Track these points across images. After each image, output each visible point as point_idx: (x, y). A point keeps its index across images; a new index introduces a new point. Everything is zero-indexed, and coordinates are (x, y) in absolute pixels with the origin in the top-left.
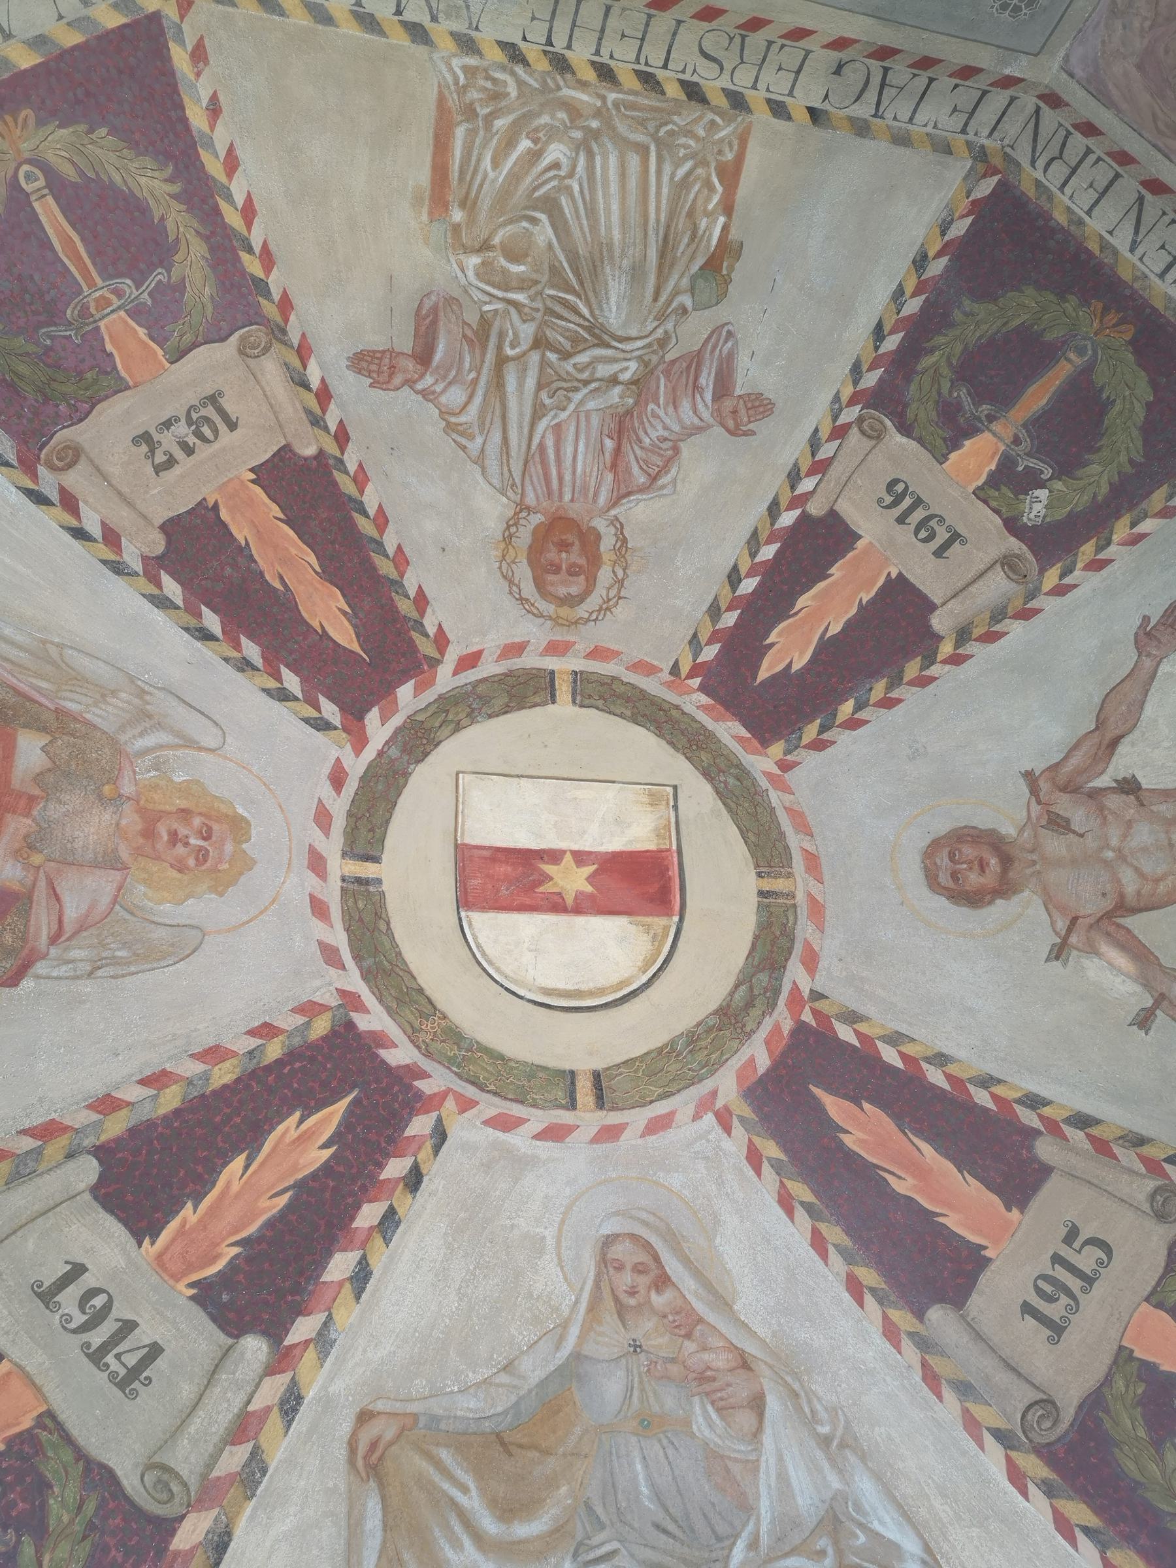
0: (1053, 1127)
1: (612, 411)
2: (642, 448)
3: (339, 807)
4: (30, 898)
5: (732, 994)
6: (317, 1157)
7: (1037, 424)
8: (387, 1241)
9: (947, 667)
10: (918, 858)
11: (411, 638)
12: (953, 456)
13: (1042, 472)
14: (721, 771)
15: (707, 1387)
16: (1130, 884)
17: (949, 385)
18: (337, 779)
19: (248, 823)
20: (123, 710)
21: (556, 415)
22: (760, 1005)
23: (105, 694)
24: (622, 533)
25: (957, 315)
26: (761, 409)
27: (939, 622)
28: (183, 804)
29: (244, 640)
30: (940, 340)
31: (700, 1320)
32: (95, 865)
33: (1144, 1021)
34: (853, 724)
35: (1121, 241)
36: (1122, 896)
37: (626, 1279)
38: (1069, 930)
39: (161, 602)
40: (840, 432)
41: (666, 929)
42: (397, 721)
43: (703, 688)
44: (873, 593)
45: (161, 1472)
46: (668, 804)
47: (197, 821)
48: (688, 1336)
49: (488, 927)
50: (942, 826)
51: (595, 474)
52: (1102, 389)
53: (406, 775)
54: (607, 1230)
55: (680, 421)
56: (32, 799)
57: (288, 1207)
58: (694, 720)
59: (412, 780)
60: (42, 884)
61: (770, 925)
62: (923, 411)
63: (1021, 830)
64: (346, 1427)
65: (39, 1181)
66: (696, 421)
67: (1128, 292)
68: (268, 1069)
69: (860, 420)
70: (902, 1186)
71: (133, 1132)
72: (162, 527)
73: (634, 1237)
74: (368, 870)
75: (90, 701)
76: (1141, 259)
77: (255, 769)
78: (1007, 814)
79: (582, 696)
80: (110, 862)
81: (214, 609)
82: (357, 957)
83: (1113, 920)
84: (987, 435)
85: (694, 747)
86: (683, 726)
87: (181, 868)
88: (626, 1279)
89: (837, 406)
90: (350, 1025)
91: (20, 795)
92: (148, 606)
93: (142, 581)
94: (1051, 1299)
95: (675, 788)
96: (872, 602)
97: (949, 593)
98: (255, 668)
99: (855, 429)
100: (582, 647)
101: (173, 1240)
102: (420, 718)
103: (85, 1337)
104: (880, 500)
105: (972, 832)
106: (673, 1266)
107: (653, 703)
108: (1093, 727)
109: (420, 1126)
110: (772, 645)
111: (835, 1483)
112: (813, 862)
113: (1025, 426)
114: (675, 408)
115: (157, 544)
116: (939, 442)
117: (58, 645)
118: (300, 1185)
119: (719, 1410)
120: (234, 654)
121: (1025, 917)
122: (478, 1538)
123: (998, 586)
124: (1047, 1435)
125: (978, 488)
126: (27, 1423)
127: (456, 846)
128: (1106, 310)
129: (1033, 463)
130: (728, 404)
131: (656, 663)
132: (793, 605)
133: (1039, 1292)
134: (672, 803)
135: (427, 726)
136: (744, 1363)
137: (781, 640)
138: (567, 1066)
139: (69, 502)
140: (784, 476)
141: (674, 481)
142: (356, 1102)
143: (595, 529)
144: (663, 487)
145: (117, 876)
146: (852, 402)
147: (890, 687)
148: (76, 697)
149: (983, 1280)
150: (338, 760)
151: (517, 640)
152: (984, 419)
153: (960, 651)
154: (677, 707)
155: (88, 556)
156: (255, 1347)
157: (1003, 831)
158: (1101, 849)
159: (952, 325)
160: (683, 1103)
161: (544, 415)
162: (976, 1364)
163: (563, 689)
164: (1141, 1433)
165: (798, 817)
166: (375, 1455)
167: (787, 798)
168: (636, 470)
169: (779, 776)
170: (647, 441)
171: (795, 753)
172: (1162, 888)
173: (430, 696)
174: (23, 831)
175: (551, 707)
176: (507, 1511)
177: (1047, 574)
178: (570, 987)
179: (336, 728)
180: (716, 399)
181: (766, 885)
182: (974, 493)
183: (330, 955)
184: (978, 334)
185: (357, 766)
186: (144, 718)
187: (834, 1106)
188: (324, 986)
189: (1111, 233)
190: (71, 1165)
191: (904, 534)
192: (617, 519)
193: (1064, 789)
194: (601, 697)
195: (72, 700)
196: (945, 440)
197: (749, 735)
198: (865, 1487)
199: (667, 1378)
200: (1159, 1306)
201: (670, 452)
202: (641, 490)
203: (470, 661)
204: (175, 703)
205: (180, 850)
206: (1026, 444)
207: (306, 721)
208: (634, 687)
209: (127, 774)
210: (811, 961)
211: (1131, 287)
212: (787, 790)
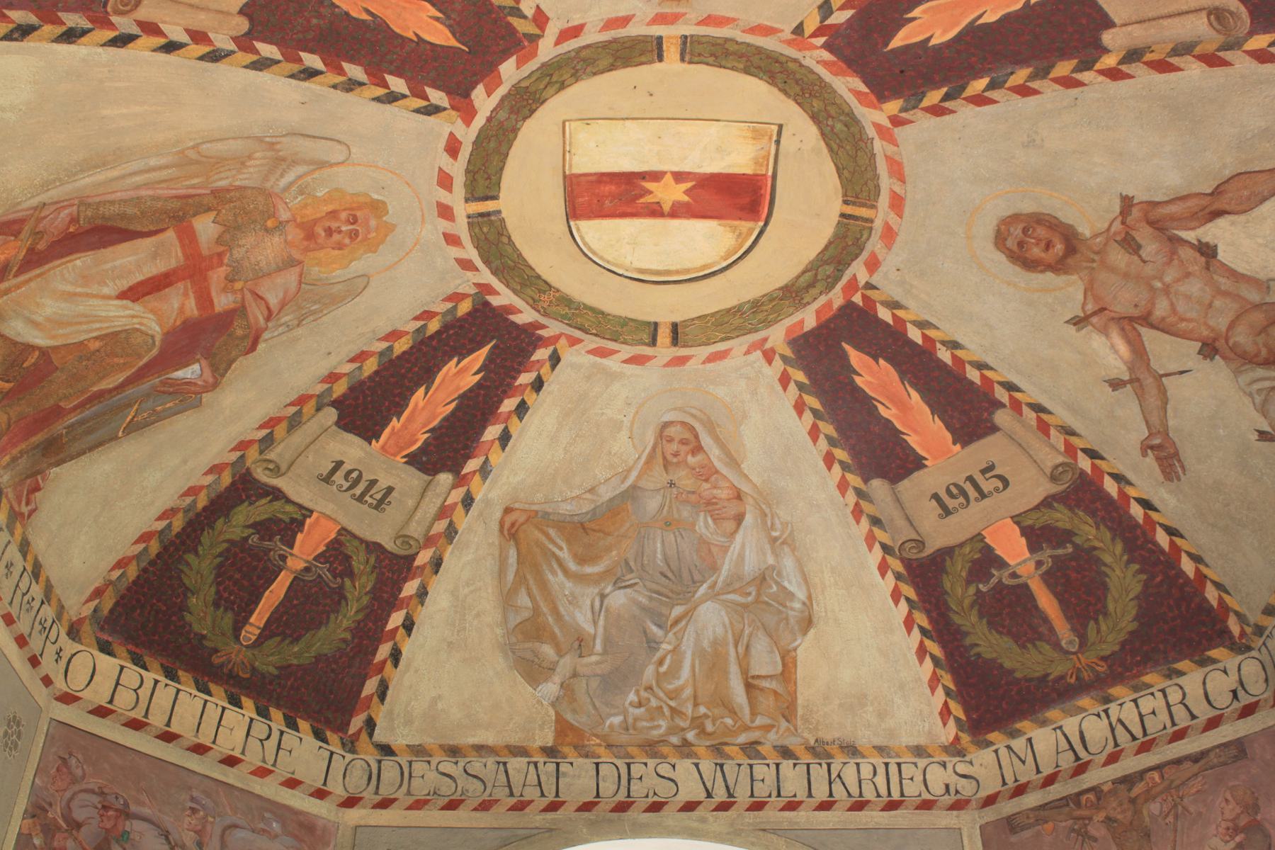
0: (1016, 406)
3: (457, 169)
4: (244, 307)
5: (798, 277)
6: (471, 380)
8: (521, 419)
9: (1101, 78)
10: (995, 223)
11: (510, 24)
14: (829, 116)
15: (710, 508)
16: (1161, 309)
18: (453, 148)
19: (384, 203)
20: (262, 165)
22: (820, 286)
23: (241, 162)
28: (330, 208)
29: (346, 65)
31: (717, 472)
32: (279, 270)
33: (1116, 384)
34: (980, 100)
36: (1149, 313)
37: (674, 447)
38: (1094, 313)
39: (262, 65)
41: (751, 231)
42: (502, 91)
43: (827, 47)
45: (405, 539)
47: (343, 215)
48: (706, 480)
49: (593, 231)
50: (1027, 207)
53: (515, 131)
54: (667, 418)
56: (220, 255)
57: (453, 413)
58: (813, 72)
59: (520, 135)
60: (248, 296)
61: (845, 237)
63: (1096, 236)
64: (498, 514)
65: (305, 427)
68: (432, 337)
71: (352, 389)
72: (241, 12)
73: (683, 423)
74: (489, 206)
75: (234, 172)
77: (380, 164)
78: (1090, 218)
79: (692, 54)
80: (291, 263)
81: (311, 51)
82: (487, 262)
83: (1133, 324)
86: (798, 76)
87: (340, 246)
88: (674, 447)
90: (487, 304)
91: (211, 257)
92: (252, 74)
93: (240, 55)
94: (952, 496)
95: (781, 127)
98: (361, 84)
100: (693, 16)
101: (389, 438)
102: (523, 84)
103: (352, 492)
105: (1052, 220)
106: (706, 440)
107: (768, 57)
108: (1209, 191)
109: (542, 354)
110: (914, 19)
111: (771, 560)
112: (897, 203)
115: (243, 25)
117: (193, 147)
118: (463, 397)
119: (714, 520)
120: (340, 79)
122: (566, 571)
124: (913, 555)
126: (333, 536)
127: (565, 177)
131: (776, 26)
133: (948, 491)
134: (775, 138)
135: (532, 89)
136: (739, 496)
137: (926, 16)
138: (653, 320)
139: (151, 28)
142: (494, 347)
145: (297, 270)
147: (1032, 77)
148: (223, 175)
149: (916, 474)
150: (451, 134)
151: (621, 14)
153: (1124, 68)
154: (795, 61)
155: (186, 61)
156: (445, 478)
157: (1080, 230)
158: (1155, 278)
160: (739, 345)
163: (671, 51)
164: (964, 574)
166: (515, 527)
167: (890, 149)
172: (1183, 325)
173: (533, 65)
174: (223, 276)
175: (658, 65)
176: (582, 561)
178: (660, 268)
179: (445, 109)
181: (849, 210)
183: (466, 265)
185: (468, 135)
186: (280, 162)
187: (855, 357)
188: (465, 283)
190: (321, 414)
193: (1151, 223)
194: (712, 55)
195: (221, 179)
197: (867, 90)
198: (788, 563)
199: (687, 502)
200: (1017, 523)
203: (575, 31)
204: (301, 141)
205: (336, 237)
207: (418, 111)
208: (748, 45)
209: (281, 207)
210: (873, 265)
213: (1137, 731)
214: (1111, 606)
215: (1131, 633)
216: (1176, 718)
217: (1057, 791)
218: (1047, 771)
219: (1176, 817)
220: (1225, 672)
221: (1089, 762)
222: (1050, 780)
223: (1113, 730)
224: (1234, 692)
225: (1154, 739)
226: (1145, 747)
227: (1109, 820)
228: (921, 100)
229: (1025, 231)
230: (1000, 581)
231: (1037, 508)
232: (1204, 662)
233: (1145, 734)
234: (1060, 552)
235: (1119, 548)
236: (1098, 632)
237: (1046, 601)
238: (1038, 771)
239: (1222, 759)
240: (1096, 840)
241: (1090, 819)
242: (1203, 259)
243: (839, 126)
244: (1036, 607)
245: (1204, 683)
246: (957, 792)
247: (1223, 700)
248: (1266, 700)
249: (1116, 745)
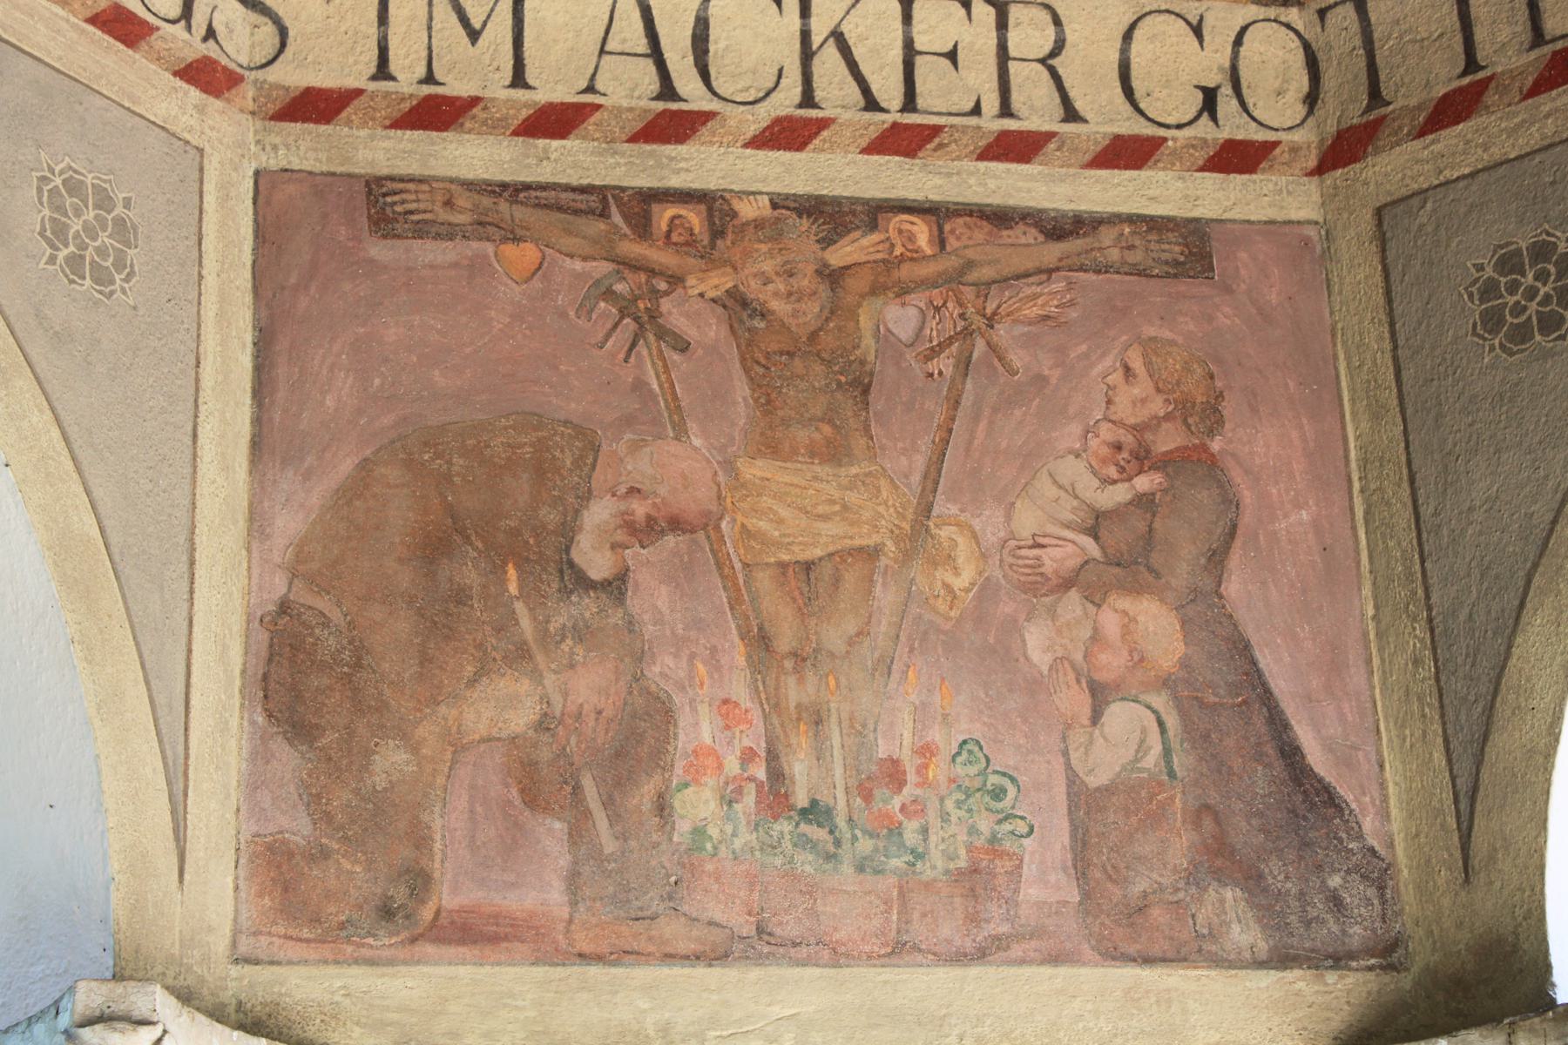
213: (888, 89)
217: (567, 161)
218: (553, 85)
219: (964, 365)
220: (1197, 31)
221: (707, 116)
222: (555, 121)
223: (807, 55)
224: (1210, 99)
225: (936, 130)
226: (903, 141)
227: (737, 304)
233: (910, 104)
238: (519, 79)
239: (1136, 257)
240: (683, 347)
241: (676, 280)
245: (1128, 36)
246: (210, 34)
247: (1172, 102)
248: (1294, 149)
249: (808, 100)
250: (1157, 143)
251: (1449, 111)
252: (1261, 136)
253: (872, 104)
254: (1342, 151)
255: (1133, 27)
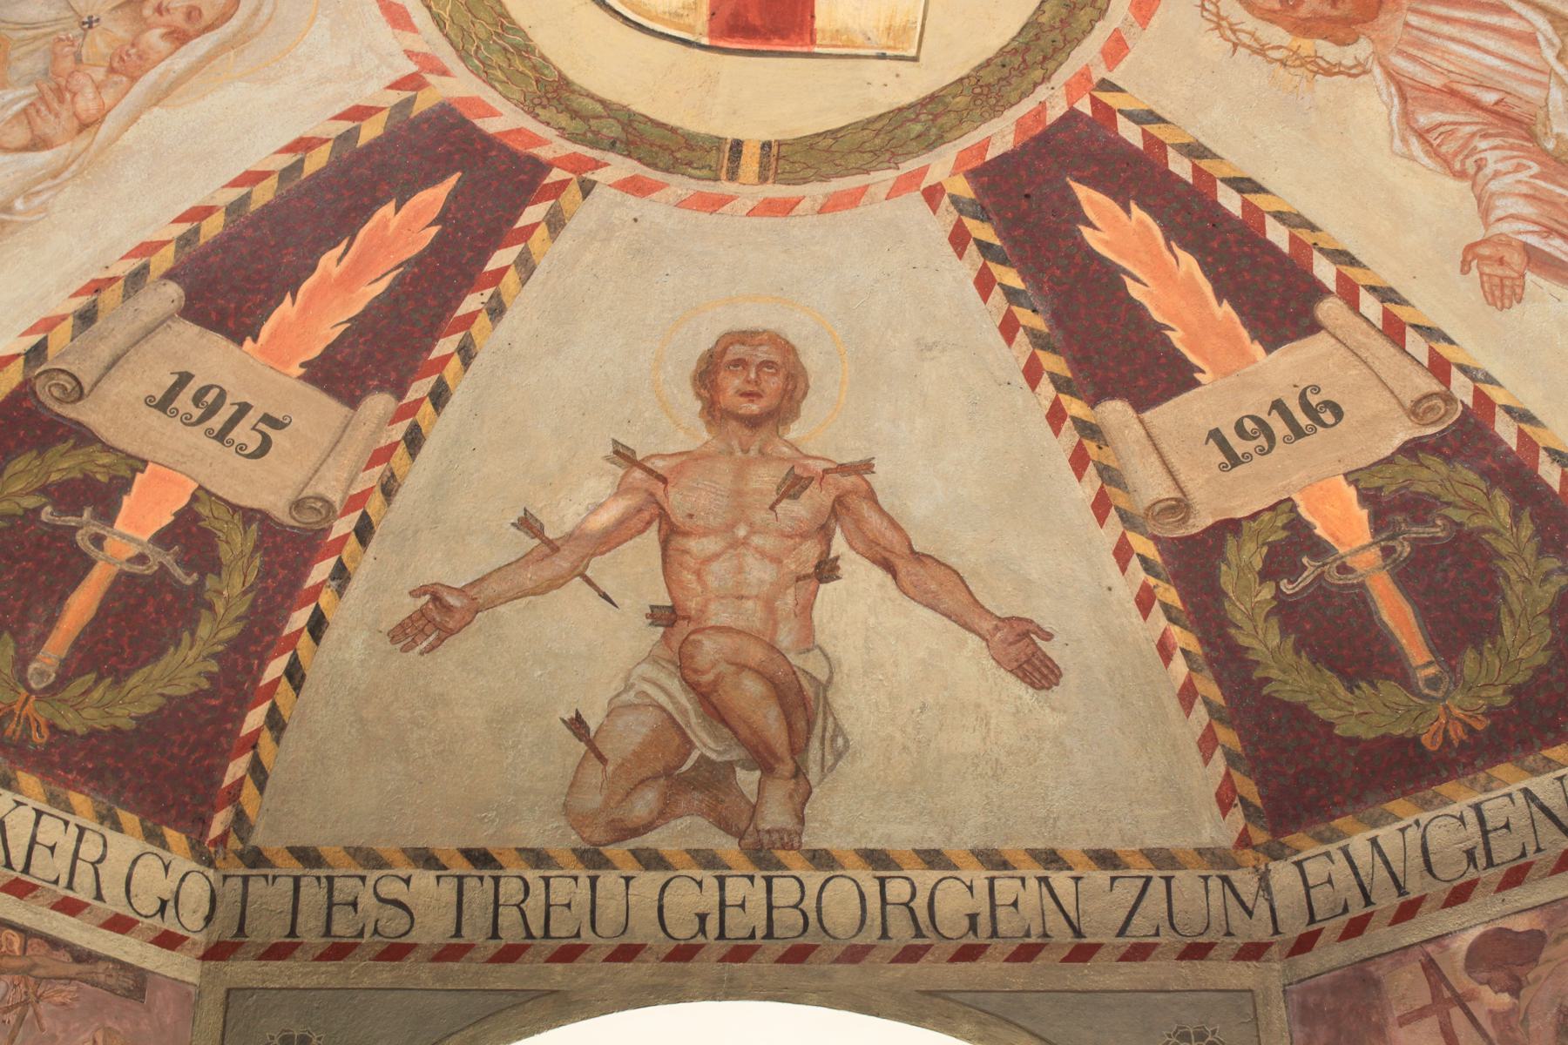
1: (1541, 114)
2: (1473, 135)
5: (592, 97)
7: (1359, 601)
10: (772, 327)
12: (1352, 492)
13: (1290, 582)
14: (936, 117)
15: (50, 97)
17: (1457, 519)
21: (1549, 41)
22: (577, 126)
24: (1340, 73)
25: (1552, 563)
26: (1497, 293)
27: (1115, 412)
30: (1527, 529)
31: (134, 80)
33: (528, 524)
35: (1544, 786)
36: (686, 534)
40: (1439, 368)
41: (690, 29)
43: (1072, 116)
44: (1178, 345)
46: (889, 48)
48: (112, 70)
50: (812, 360)
51: (1445, 65)
52: (1374, 686)
55: (1503, 194)
58: (1024, 95)
61: (691, 148)
62: (1430, 476)
63: (791, 445)
66: (1499, 213)
67: (1479, 763)
69: (1449, 399)
70: (329, 262)
76: (1509, 795)
78: (817, 432)
84: (1367, 538)
85: (978, 90)
89: (1480, 376)
94: (197, 399)
95: (915, 59)
96: (1167, 342)
97: (1155, 432)
99: (1436, 387)
104: (1316, 389)
106: (201, 46)
108: (917, 548)
110: (1128, 211)
113: (1362, 585)
114: (1526, 196)
116: (1378, 482)
119: (24, 111)
121: (675, 427)
123: (1150, 486)
124: (46, 394)
125: (1294, 508)
128: (1471, 730)
129: (1307, 577)
130: (1516, 259)
132: (1185, 247)
133: (205, 390)
134: (889, 53)
137: (1133, 223)
140: (1393, 284)
141: (1413, 159)
143: (1356, 41)
144: (1404, 140)
146: (1479, 395)
152: (1391, 543)
153: (1068, 422)
154: (1046, 78)
157: (795, 426)
158: (751, 525)
159: (1541, 552)
161: (1556, 29)
162: (117, 326)
164: (55, 477)
165: (853, 199)
167: (883, 191)
168: (1439, 117)
169: (918, 185)
170: (1483, 145)
171: (952, 208)
172: (689, 577)
177: (1151, 543)
180: (1525, 246)
182: (1289, 499)
184: (1513, 577)
187: (434, 197)
189: (1560, 779)
191: (1257, 403)
192: (1365, 72)
193: (839, 500)
196: (1380, 489)
197: (988, 157)
199: (55, 57)
201: (1457, 166)
202: (1406, 116)
206: (1335, 578)
210: (634, 186)
211: (1482, 769)
212: (895, 191)
213: (18, 859)
214: (135, 679)
215: (116, 730)
216: (76, 880)
219: (21, 1019)
220: (166, 868)
224: (164, 903)
225: (35, 887)
228: (975, 217)
229: (768, 364)
230: (75, 529)
231: (235, 508)
232: (153, 836)
233: (26, 870)
234: (178, 572)
235: (232, 632)
236: (86, 693)
237: (82, 604)
239: (111, 981)
242: (811, 570)
243: (918, 128)
244: (63, 598)
245: (135, 862)
247: (147, 905)
248: (194, 943)
250: (134, 923)
251: (277, 952)
252: (182, 932)
253: (9, 865)
254: (217, 952)
255: (138, 858)
